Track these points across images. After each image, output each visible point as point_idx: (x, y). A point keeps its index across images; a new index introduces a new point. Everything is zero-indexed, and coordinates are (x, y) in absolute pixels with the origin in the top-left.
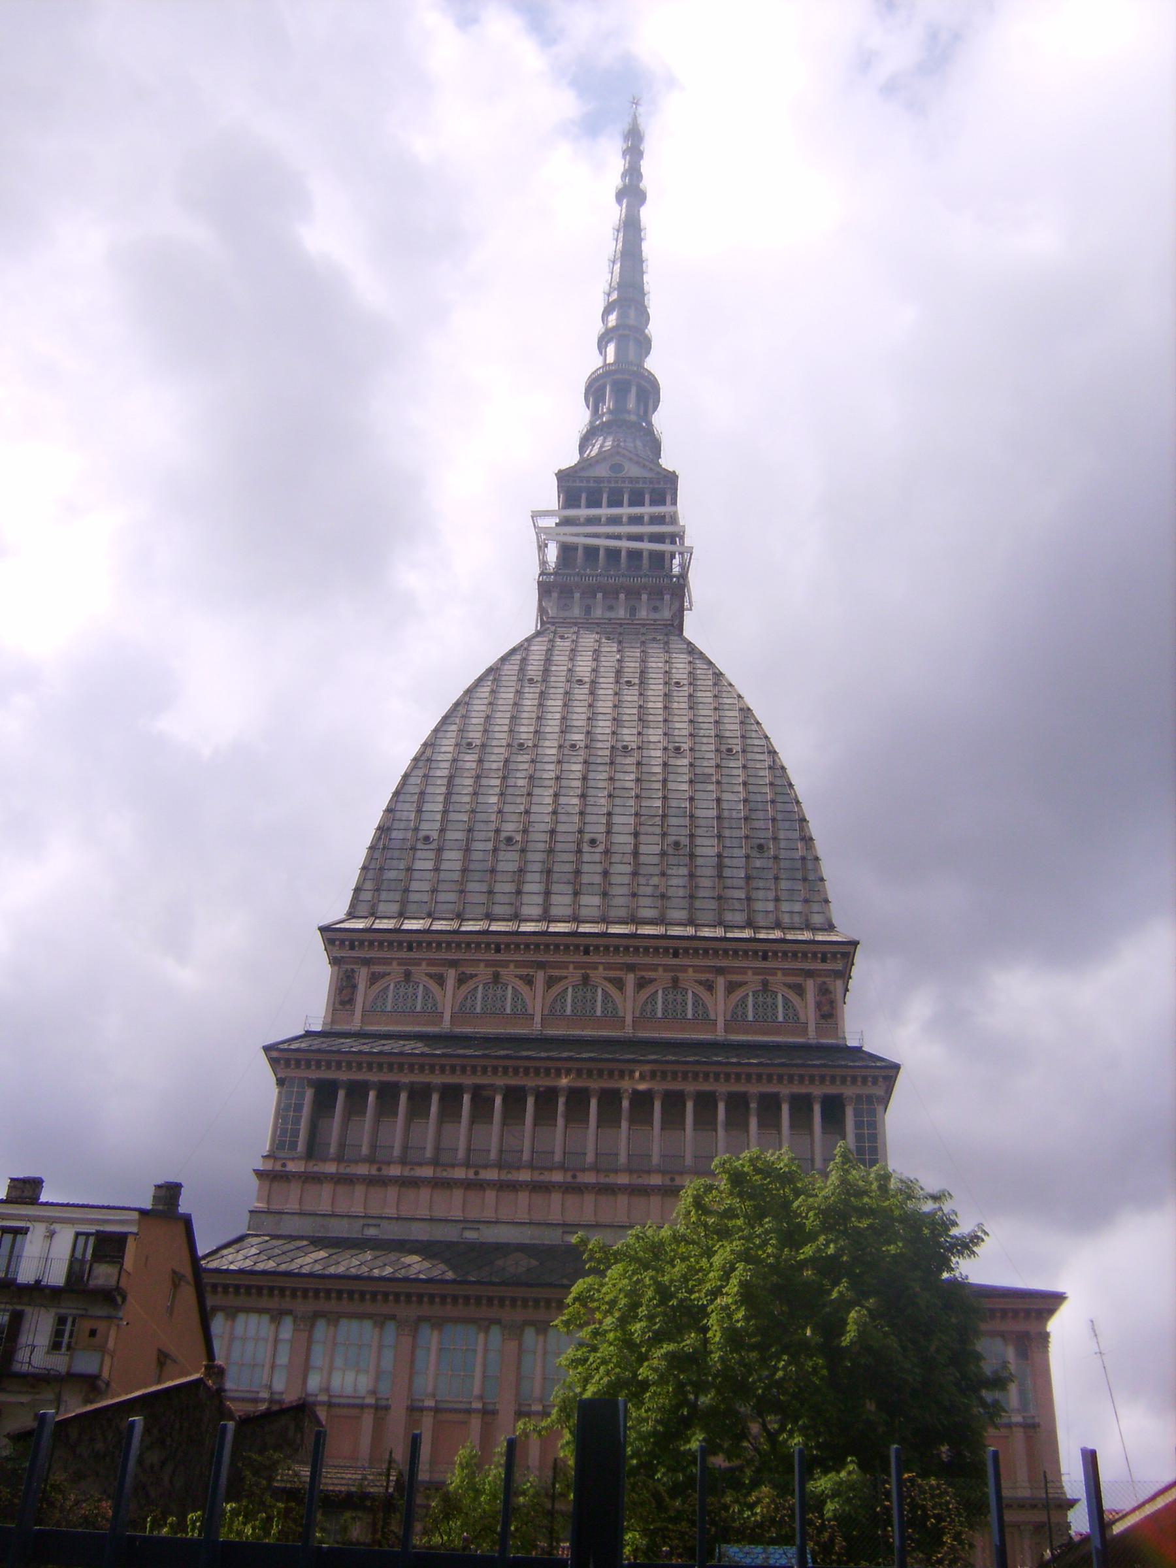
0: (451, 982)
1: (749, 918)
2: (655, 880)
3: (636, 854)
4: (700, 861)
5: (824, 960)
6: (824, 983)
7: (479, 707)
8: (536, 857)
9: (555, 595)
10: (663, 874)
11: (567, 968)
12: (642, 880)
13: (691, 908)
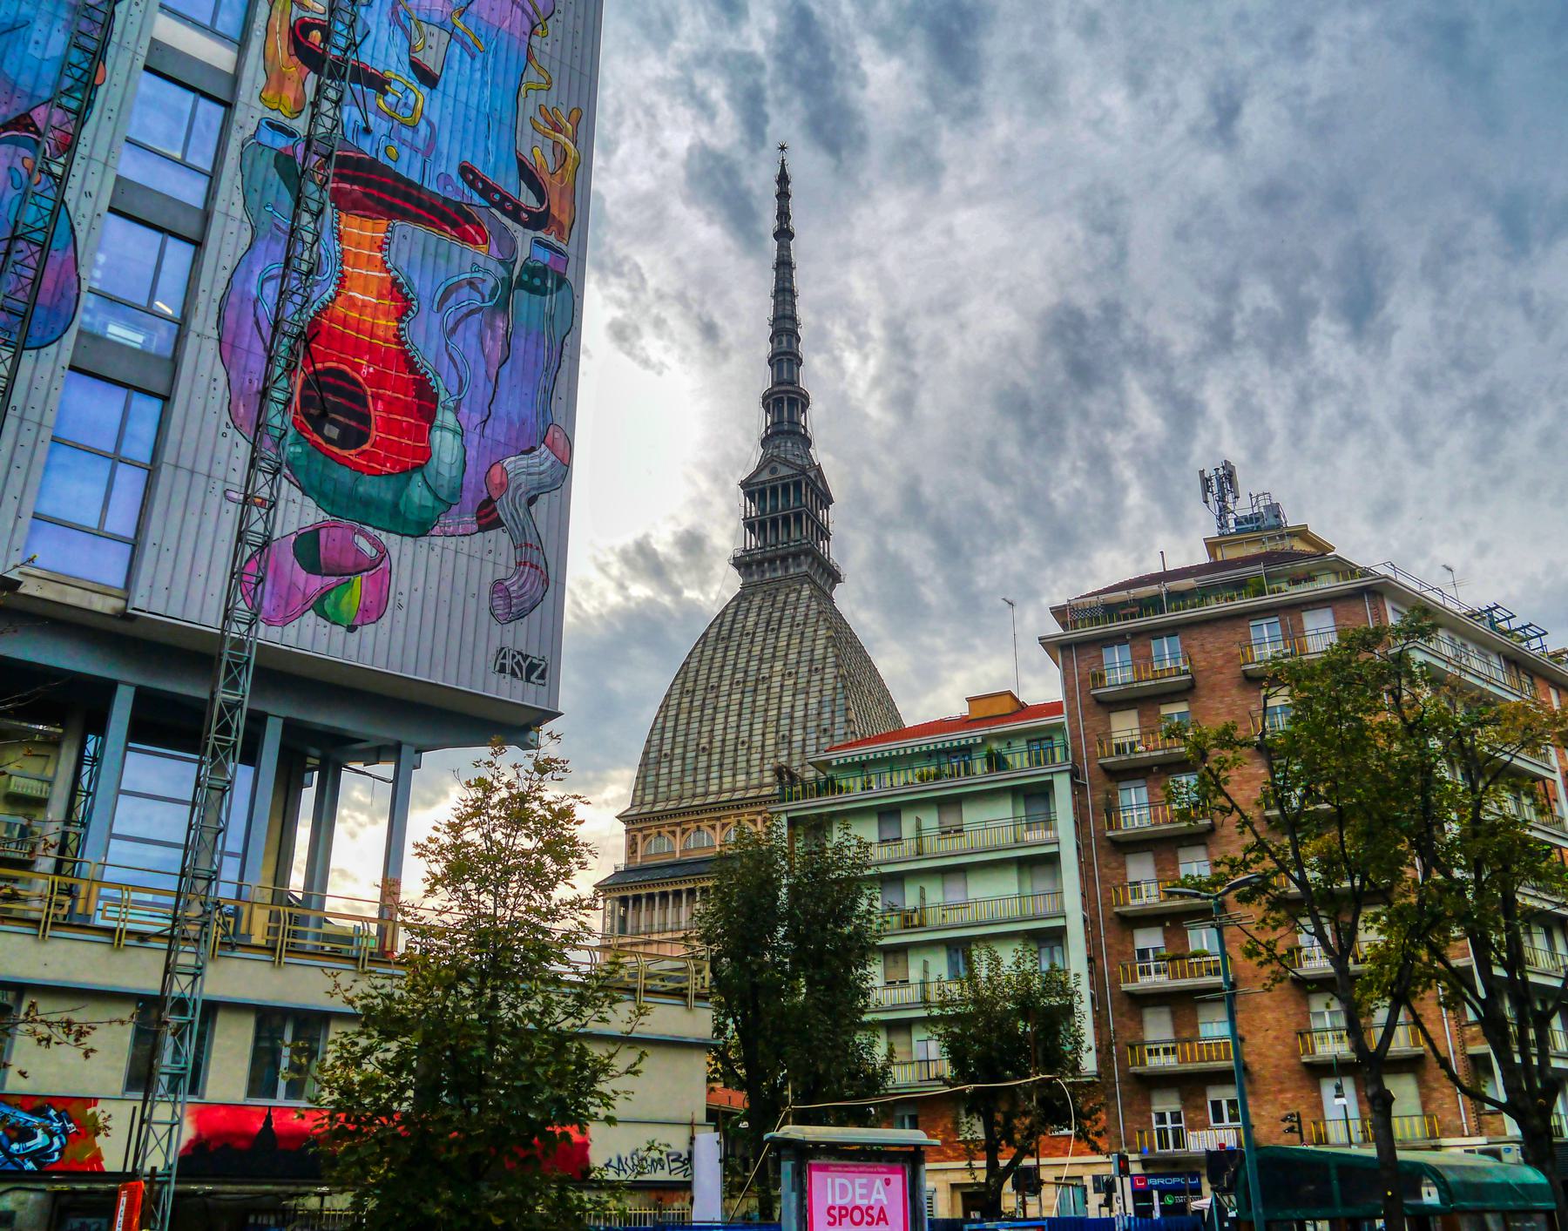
0: (678, 834)
3: (763, 746)
4: (794, 745)
7: (694, 665)
8: (716, 757)
10: (776, 756)
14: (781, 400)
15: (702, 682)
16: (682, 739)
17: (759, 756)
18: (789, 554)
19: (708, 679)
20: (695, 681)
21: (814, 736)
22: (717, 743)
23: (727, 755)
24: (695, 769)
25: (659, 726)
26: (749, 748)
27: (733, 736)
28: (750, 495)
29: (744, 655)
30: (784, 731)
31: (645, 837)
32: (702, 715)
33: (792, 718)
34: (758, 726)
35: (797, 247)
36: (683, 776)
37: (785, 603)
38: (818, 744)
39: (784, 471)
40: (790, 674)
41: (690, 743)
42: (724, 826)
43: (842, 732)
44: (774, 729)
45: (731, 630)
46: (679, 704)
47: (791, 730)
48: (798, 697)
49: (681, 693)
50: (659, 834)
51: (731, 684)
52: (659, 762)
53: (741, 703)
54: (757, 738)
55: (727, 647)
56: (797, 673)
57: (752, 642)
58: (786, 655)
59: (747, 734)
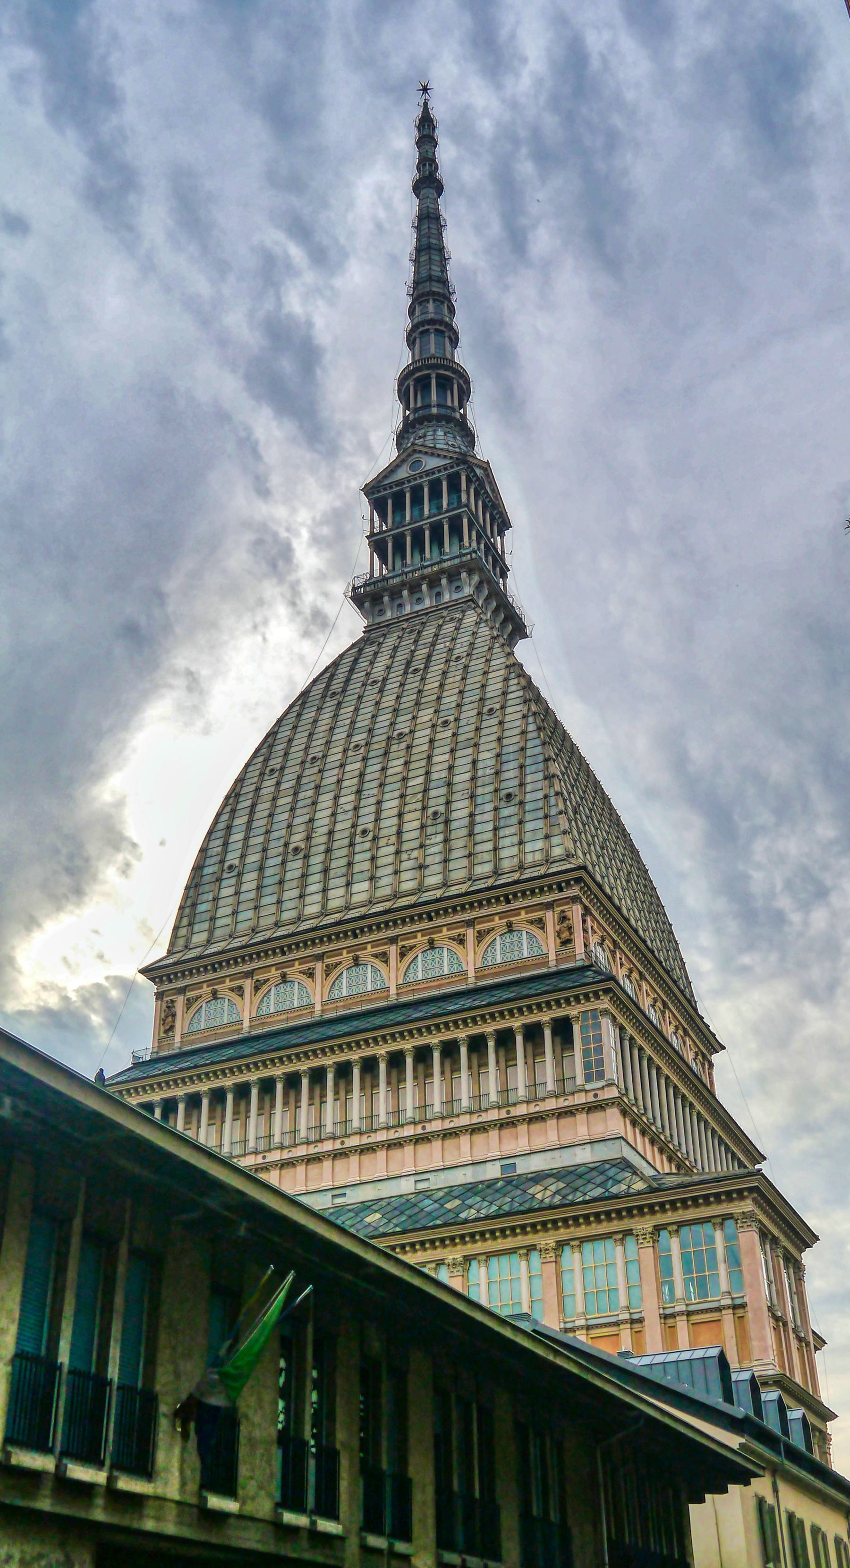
1: (495, 867)
2: (415, 854)
3: (399, 833)
5: (561, 889)
6: (563, 911)
7: (285, 733)
8: (317, 860)
9: (367, 605)
11: (341, 954)
12: (404, 856)
13: (446, 871)
14: (428, 377)
15: (296, 754)
16: (261, 839)
17: (392, 849)
18: (442, 572)
19: (307, 748)
20: (286, 754)
21: (489, 807)
22: (320, 839)
23: (336, 854)
24: (281, 882)
25: (221, 826)
26: (375, 838)
27: (348, 824)
28: (378, 505)
29: (367, 709)
30: (437, 804)
31: (189, 1003)
32: (295, 801)
33: (449, 784)
34: (391, 805)
36: (259, 897)
37: (436, 635)
38: (496, 819)
39: (431, 463)
40: (446, 723)
41: (273, 844)
42: (328, 970)
43: (540, 795)
44: (419, 806)
45: (348, 681)
46: (258, 789)
47: (448, 803)
48: (458, 754)
49: (262, 774)
50: (215, 994)
51: (345, 751)
52: (219, 880)
53: (362, 775)
54: (389, 824)
55: (339, 704)
56: (456, 720)
57: (381, 691)
58: (439, 698)
59: (372, 818)
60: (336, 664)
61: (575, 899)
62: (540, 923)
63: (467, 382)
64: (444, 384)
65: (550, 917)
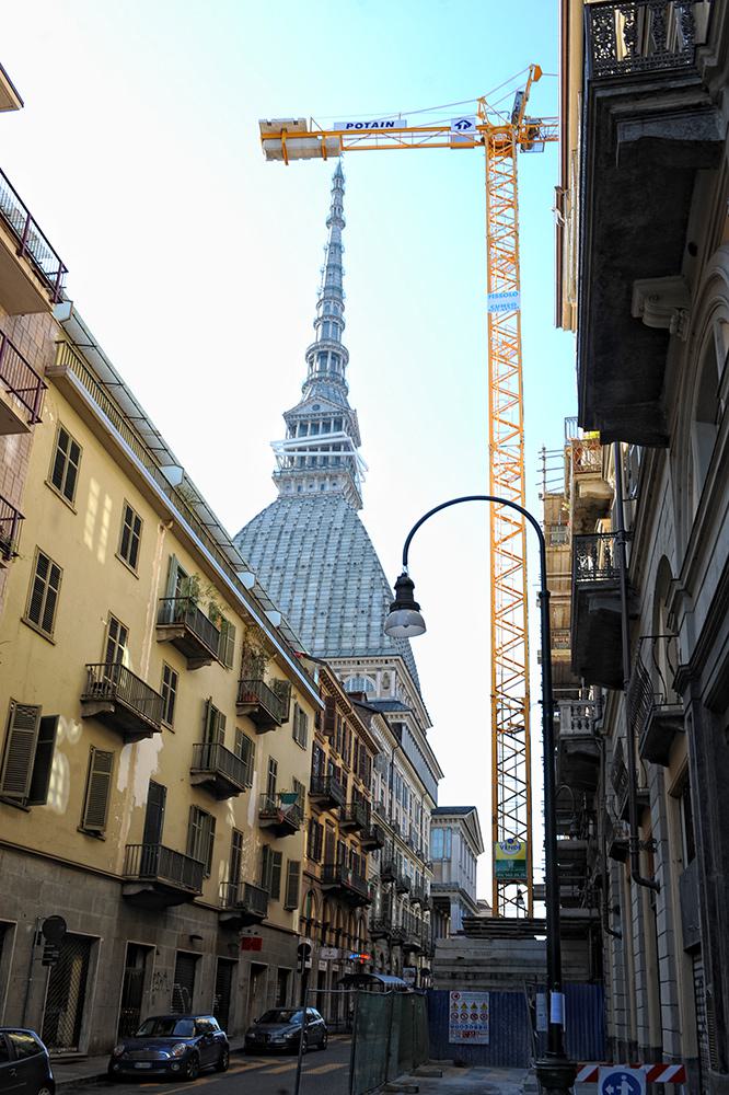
5: (386, 662)
14: (327, 352)
35: (346, 237)
60: (262, 514)
61: (393, 669)
62: (374, 676)
63: (348, 358)
64: (335, 357)
65: (380, 675)
